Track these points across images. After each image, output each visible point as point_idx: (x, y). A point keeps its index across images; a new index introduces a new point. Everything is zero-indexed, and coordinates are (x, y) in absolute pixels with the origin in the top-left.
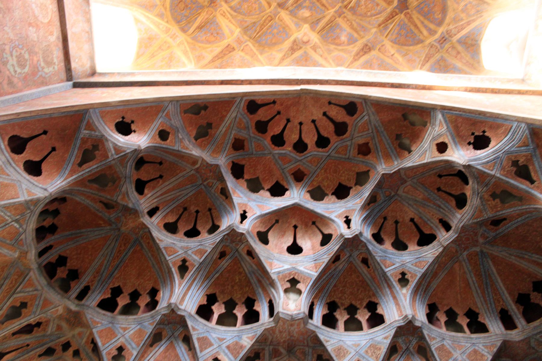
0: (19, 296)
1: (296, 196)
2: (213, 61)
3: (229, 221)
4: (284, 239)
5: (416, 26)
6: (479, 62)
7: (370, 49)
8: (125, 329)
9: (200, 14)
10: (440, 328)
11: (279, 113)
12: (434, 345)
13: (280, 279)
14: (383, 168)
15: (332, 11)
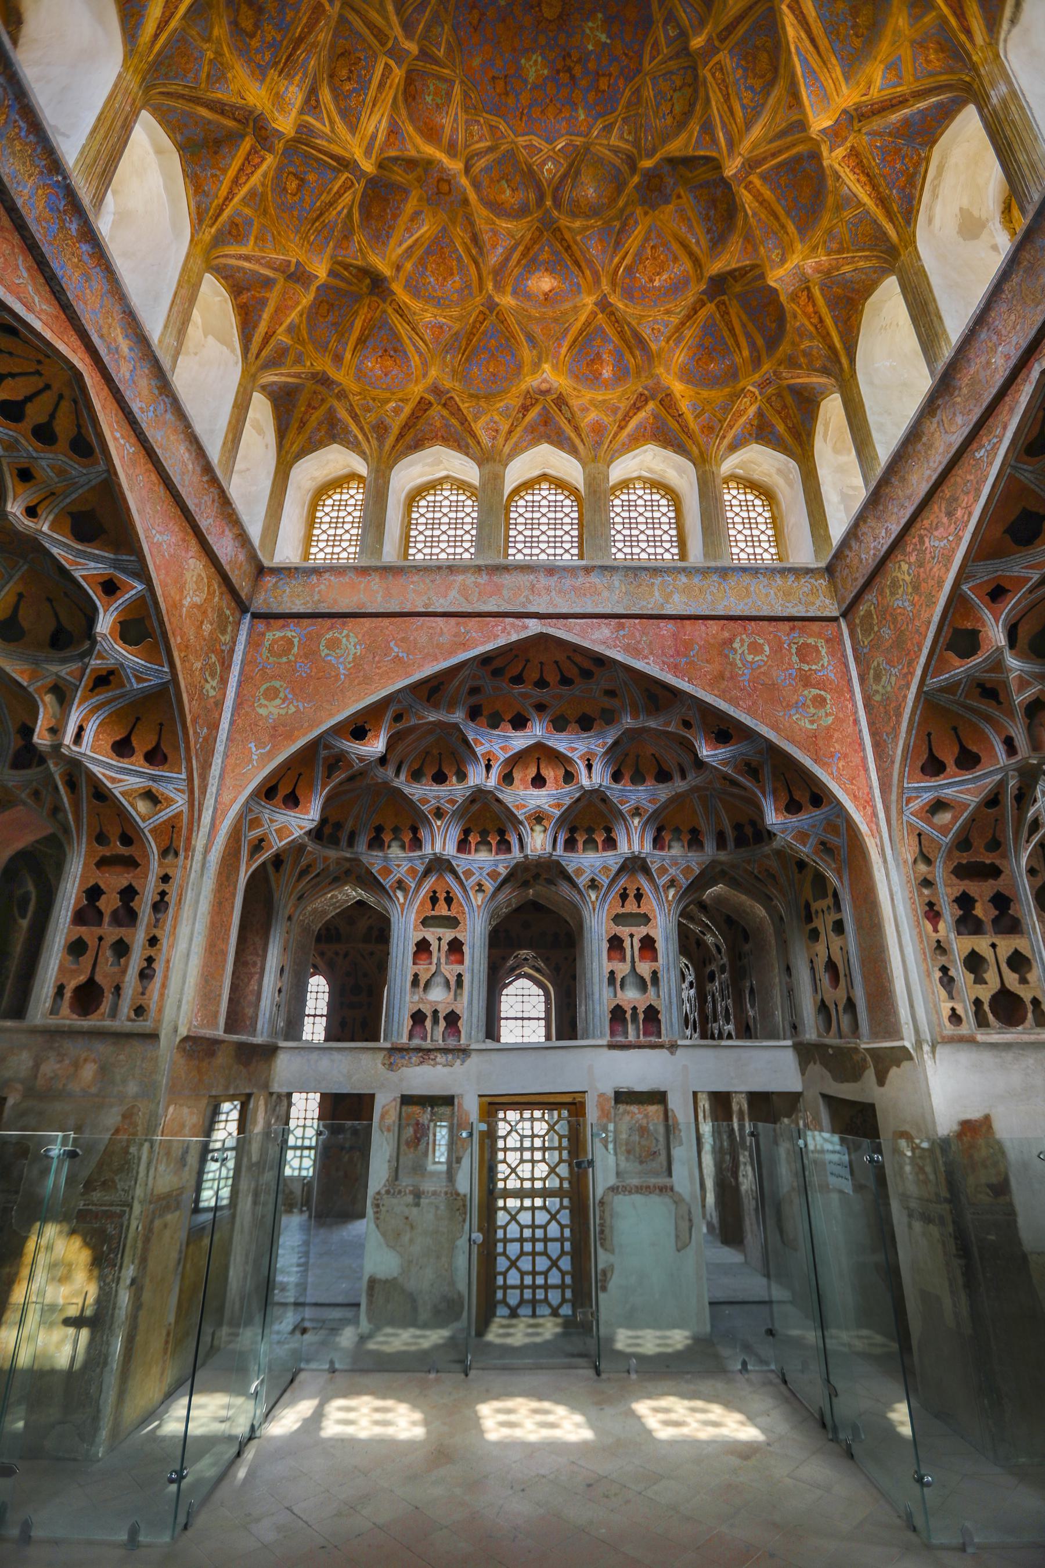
0: (304, 862)
1: (537, 731)
2: (401, 436)
3: (476, 777)
4: (529, 771)
5: (732, 330)
6: (810, 434)
7: (646, 401)
8: (399, 866)
9: (356, 312)
10: (662, 848)
11: (517, 656)
12: (654, 868)
13: (527, 818)
14: (628, 721)
15: (589, 301)
